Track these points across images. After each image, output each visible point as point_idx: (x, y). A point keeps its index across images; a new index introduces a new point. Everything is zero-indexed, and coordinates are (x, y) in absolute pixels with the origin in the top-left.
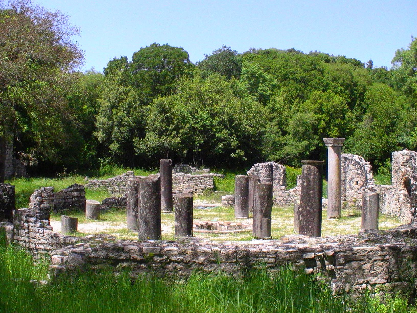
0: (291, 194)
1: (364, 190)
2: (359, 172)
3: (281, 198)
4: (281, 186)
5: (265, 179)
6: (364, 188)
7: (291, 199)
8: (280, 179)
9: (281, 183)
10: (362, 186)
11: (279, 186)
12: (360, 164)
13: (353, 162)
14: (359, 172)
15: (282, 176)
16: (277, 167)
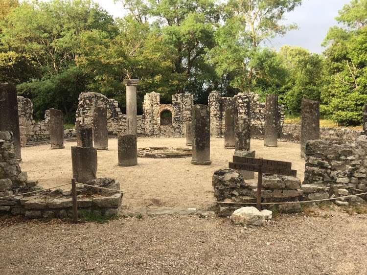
0: (42, 128)
1: (113, 120)
2: (108, 106)
3: (32, 133)
4: (31, 120)
5: (23, 113)
6: (113, 118)
7: (42, 133)
8: (31, 114)
9: (32, 118)
10: (111, 117)
11: (30, 120)
12: (108, 101)
13: (102, 99)
14: (108, 106)
15: (33, 111)
16: (27, 101)
